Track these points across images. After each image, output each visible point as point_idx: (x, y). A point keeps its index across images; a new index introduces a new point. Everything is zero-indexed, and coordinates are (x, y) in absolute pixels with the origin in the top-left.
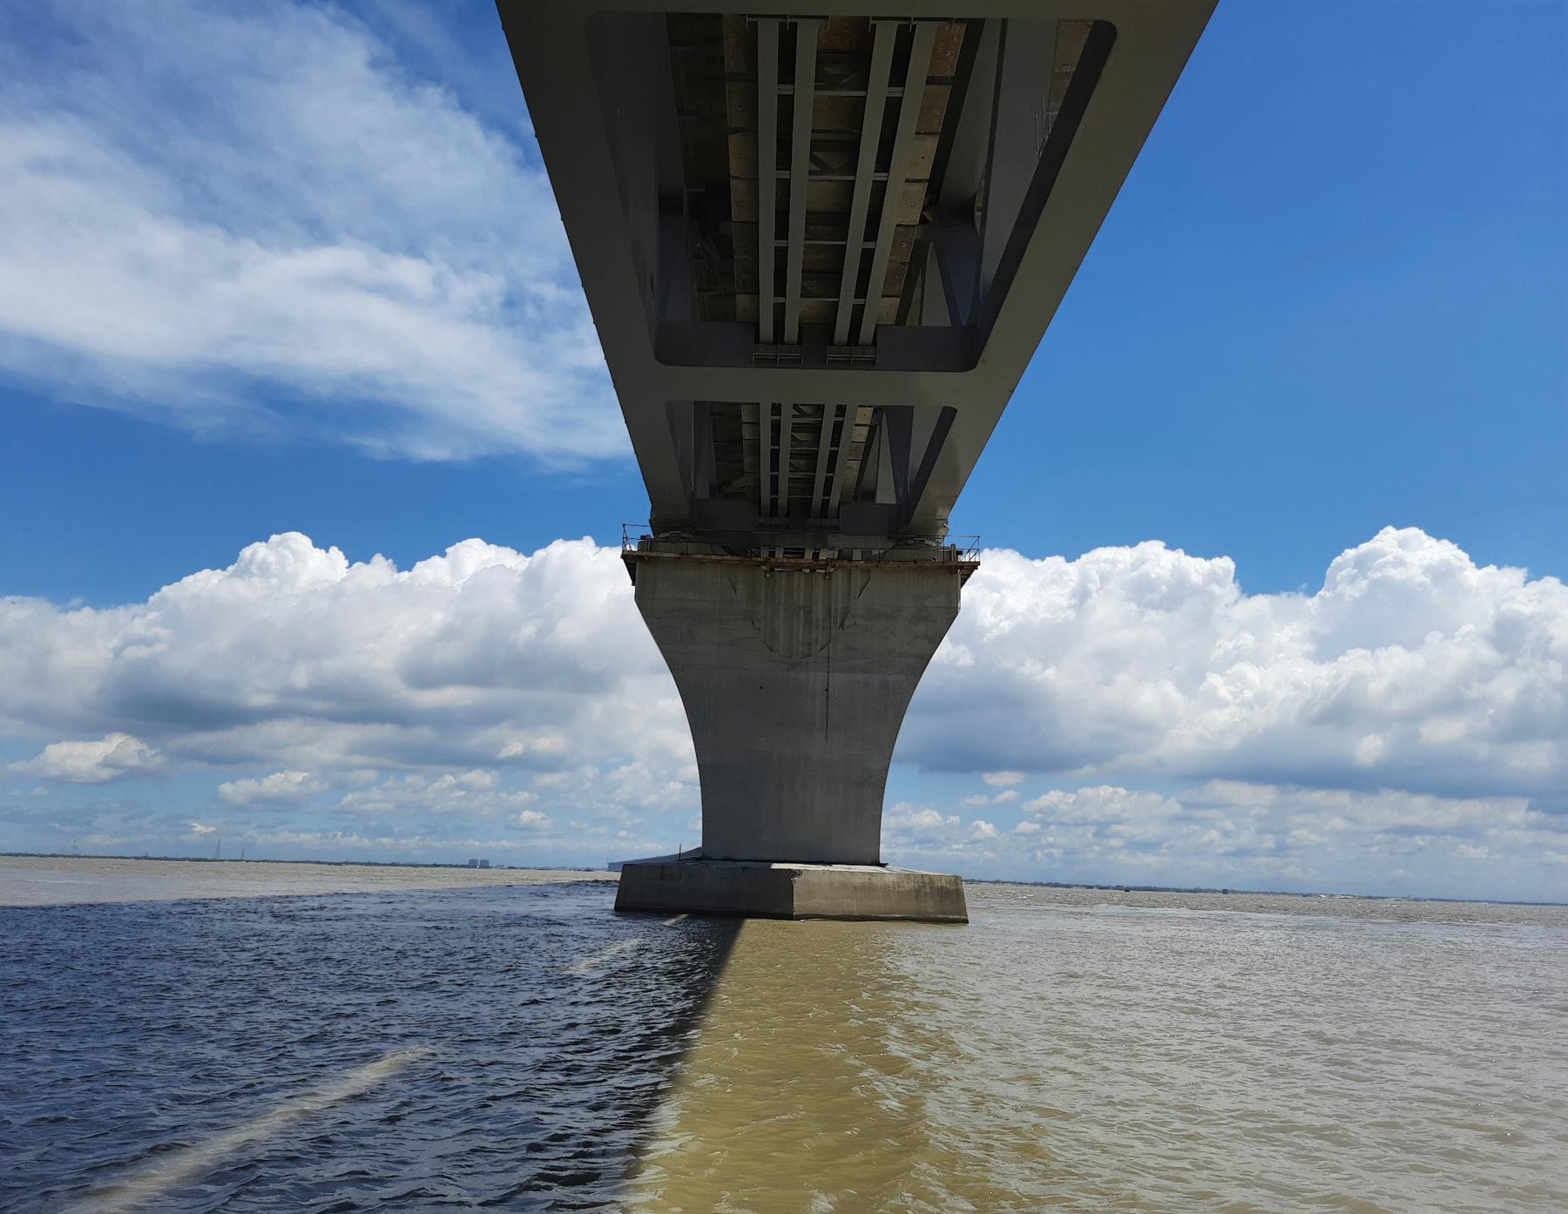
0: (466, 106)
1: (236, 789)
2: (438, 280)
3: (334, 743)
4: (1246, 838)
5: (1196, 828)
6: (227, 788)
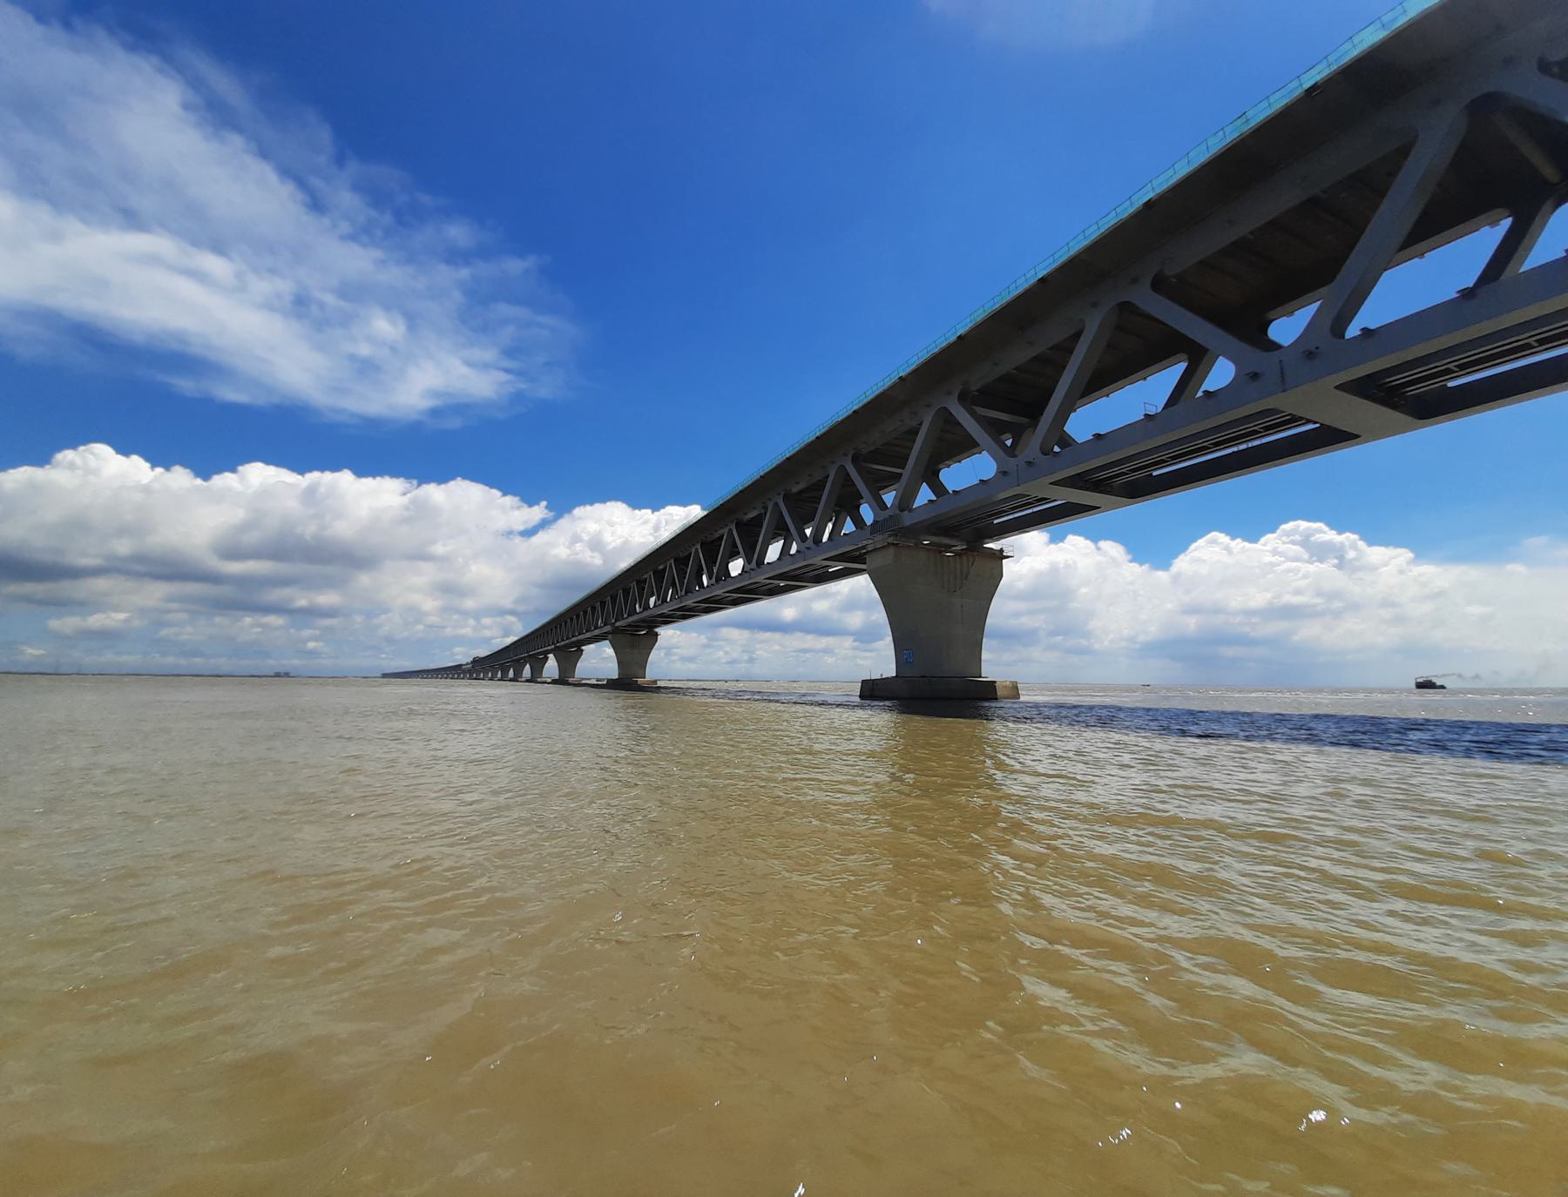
0: (264, 154)
1: (68, 623)
2: (239, 276)
3: (155, 593)
4: (735, 655)
5: (712, 650)
6: (54, 624)
